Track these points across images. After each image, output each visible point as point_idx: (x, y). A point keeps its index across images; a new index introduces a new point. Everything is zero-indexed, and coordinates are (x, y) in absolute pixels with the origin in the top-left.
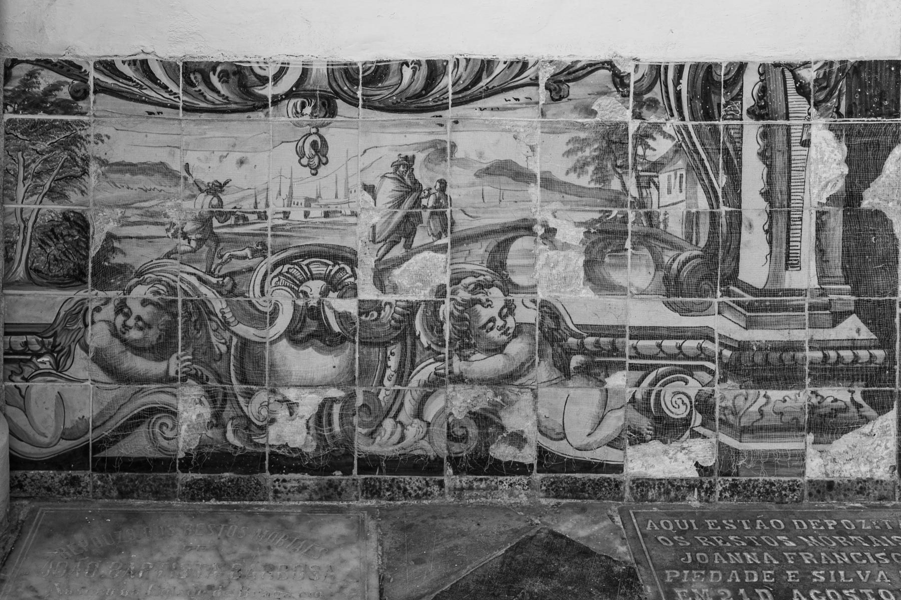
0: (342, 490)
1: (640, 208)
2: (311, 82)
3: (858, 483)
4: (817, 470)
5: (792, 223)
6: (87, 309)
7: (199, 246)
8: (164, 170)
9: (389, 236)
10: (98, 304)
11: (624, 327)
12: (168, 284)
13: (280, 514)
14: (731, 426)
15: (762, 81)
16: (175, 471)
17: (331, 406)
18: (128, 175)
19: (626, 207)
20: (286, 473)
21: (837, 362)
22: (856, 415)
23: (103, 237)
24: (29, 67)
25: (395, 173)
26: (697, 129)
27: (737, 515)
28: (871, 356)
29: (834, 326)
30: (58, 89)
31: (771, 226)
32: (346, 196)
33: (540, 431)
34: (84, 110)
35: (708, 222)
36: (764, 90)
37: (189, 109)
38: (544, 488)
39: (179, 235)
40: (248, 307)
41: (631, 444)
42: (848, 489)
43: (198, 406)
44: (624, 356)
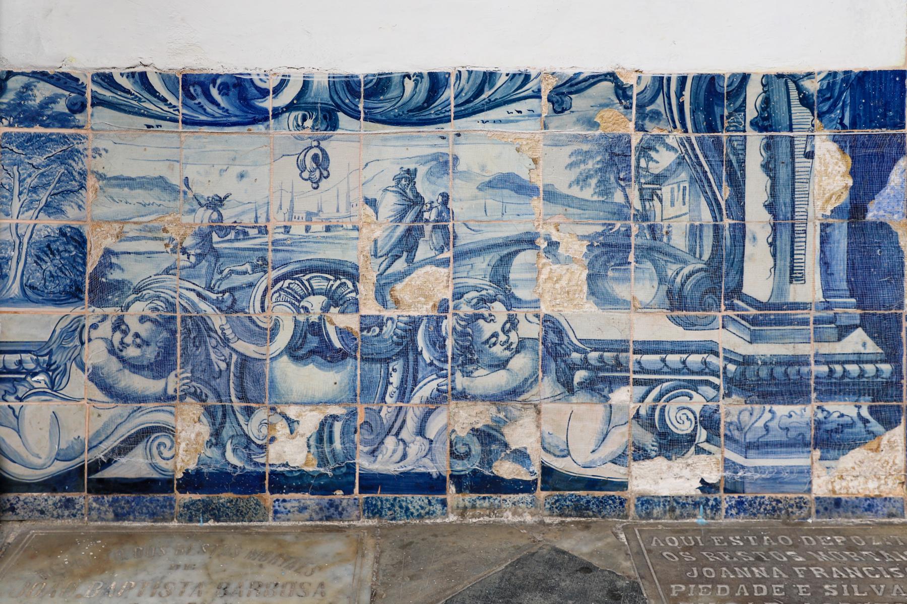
0: (343, 509)
1: (643, 221)
2: (312, 95)
3: (866, 500)
4: (824, 488)
5: (796, 236)
6: (84, 326)
7: (199, 261)
8: (164, 185)
9: (391, 250)
10: (95, 321)
11: (628, 342)
12: (167, 300)
13: (279, 534)
14: (736, 441)
15: (765, 92)
16: (173, 491)
17: (331, 426)
18: (126, 190)
19: (629, 219)
20: (286, 493)
21: (843, 377)
22: (863, 430)
23: (101, 253)
24: (25, 80)
25: (397, 186)
26: (700, 141)
27: (742, 531)
28: (878, 370)
29: (839, 340)
30: (54, 102)
31: (774, 239)
32: (348, 210)
33: (544, 448)
34: (81, 124)
35: (711, 234)
36: (767, 101)
37: (188, 122)
38: (548, 506)
39: (179, 250)
40: (248, 323)
41: (635, 460)
42: (856, 507)
43: (198, 424)
44: (628, 371)
